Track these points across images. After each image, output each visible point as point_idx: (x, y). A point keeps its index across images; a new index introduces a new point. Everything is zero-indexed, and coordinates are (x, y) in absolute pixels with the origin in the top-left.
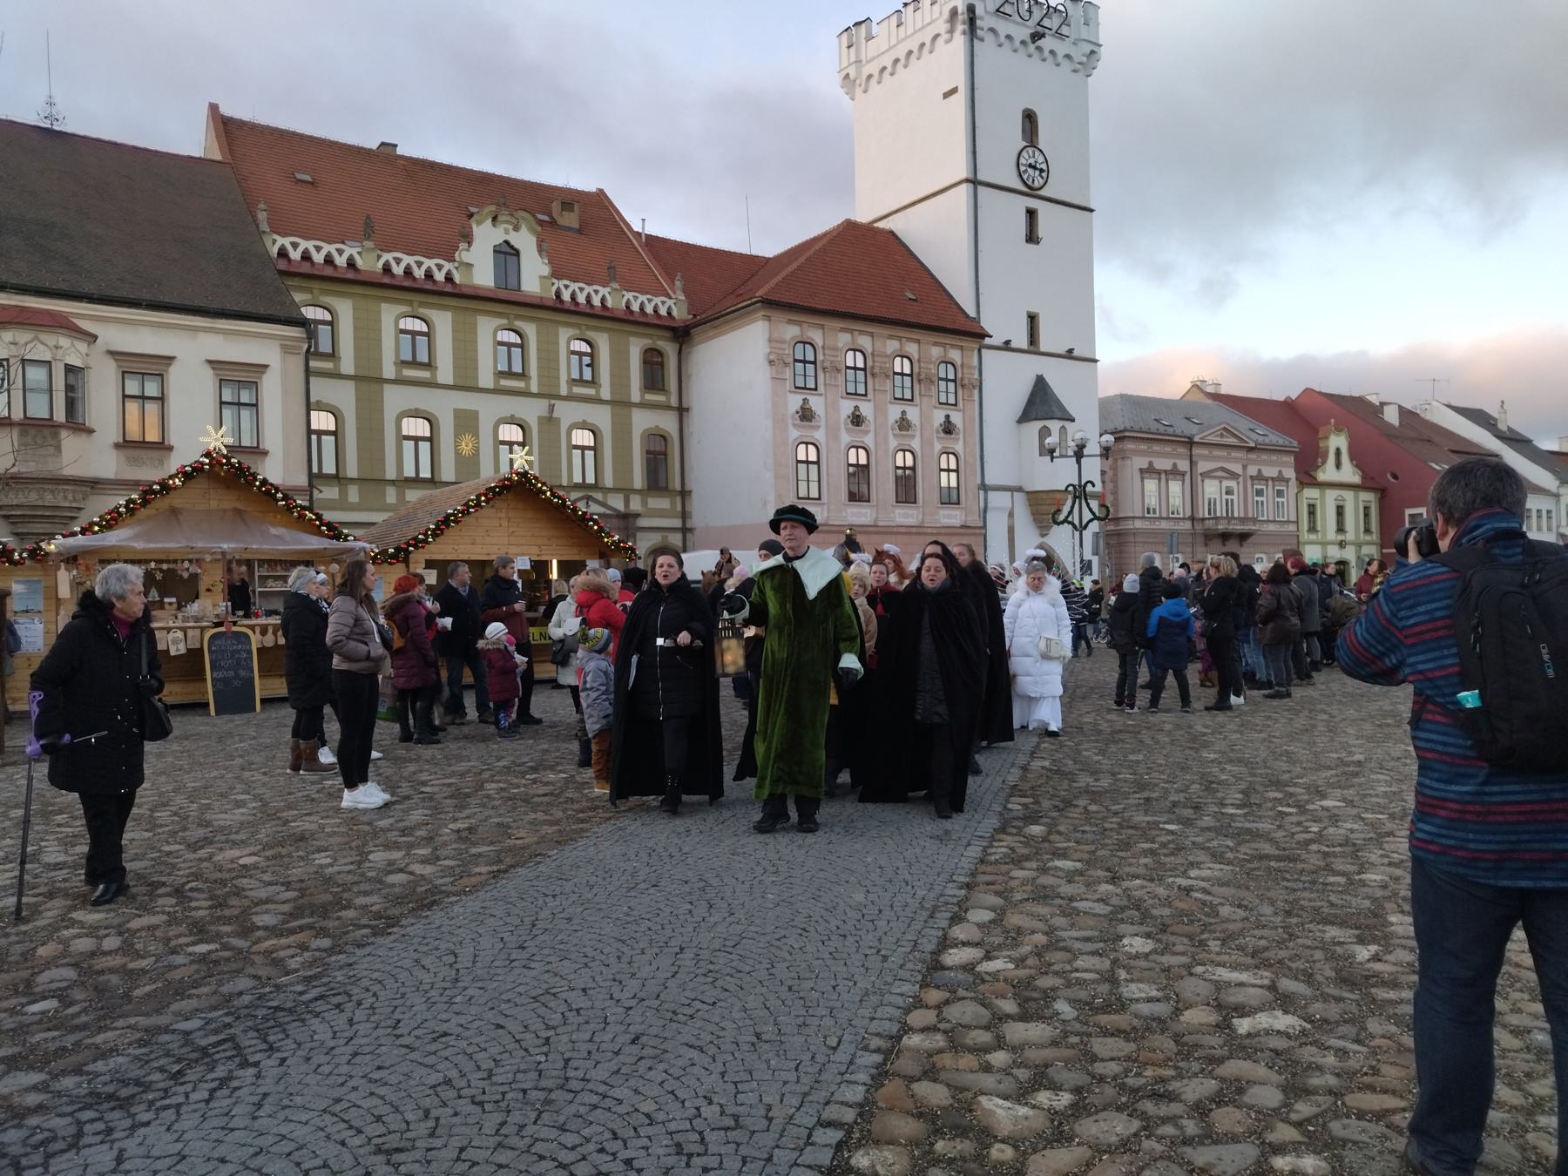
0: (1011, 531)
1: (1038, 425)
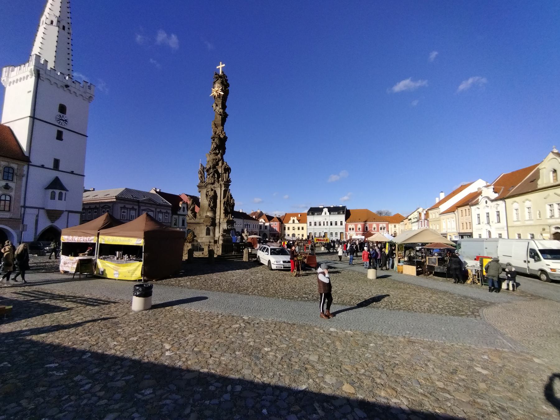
0: (37, 221)
1: (51, 191)
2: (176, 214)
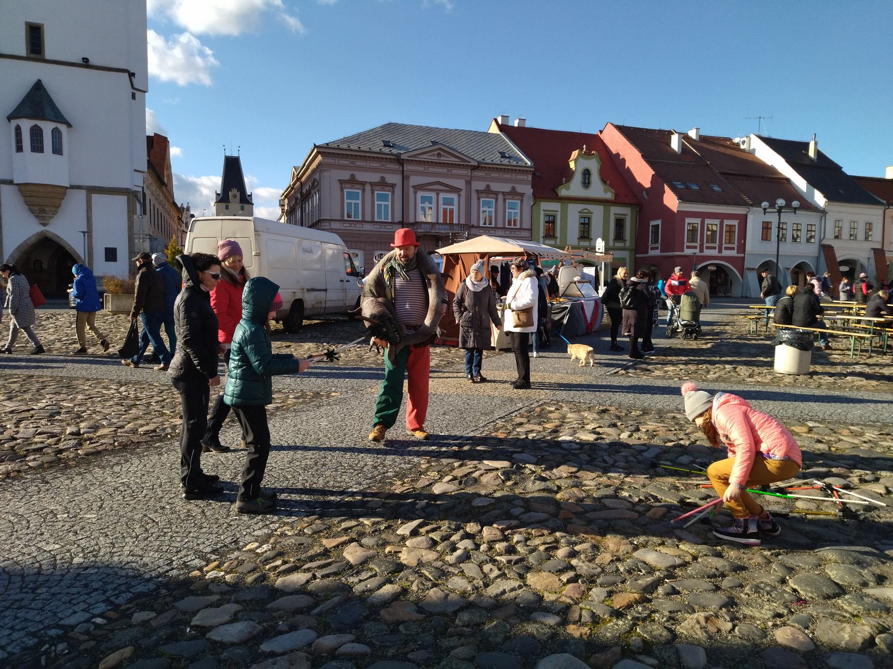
2: (554, 196)
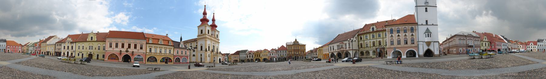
0: (423, 47)
